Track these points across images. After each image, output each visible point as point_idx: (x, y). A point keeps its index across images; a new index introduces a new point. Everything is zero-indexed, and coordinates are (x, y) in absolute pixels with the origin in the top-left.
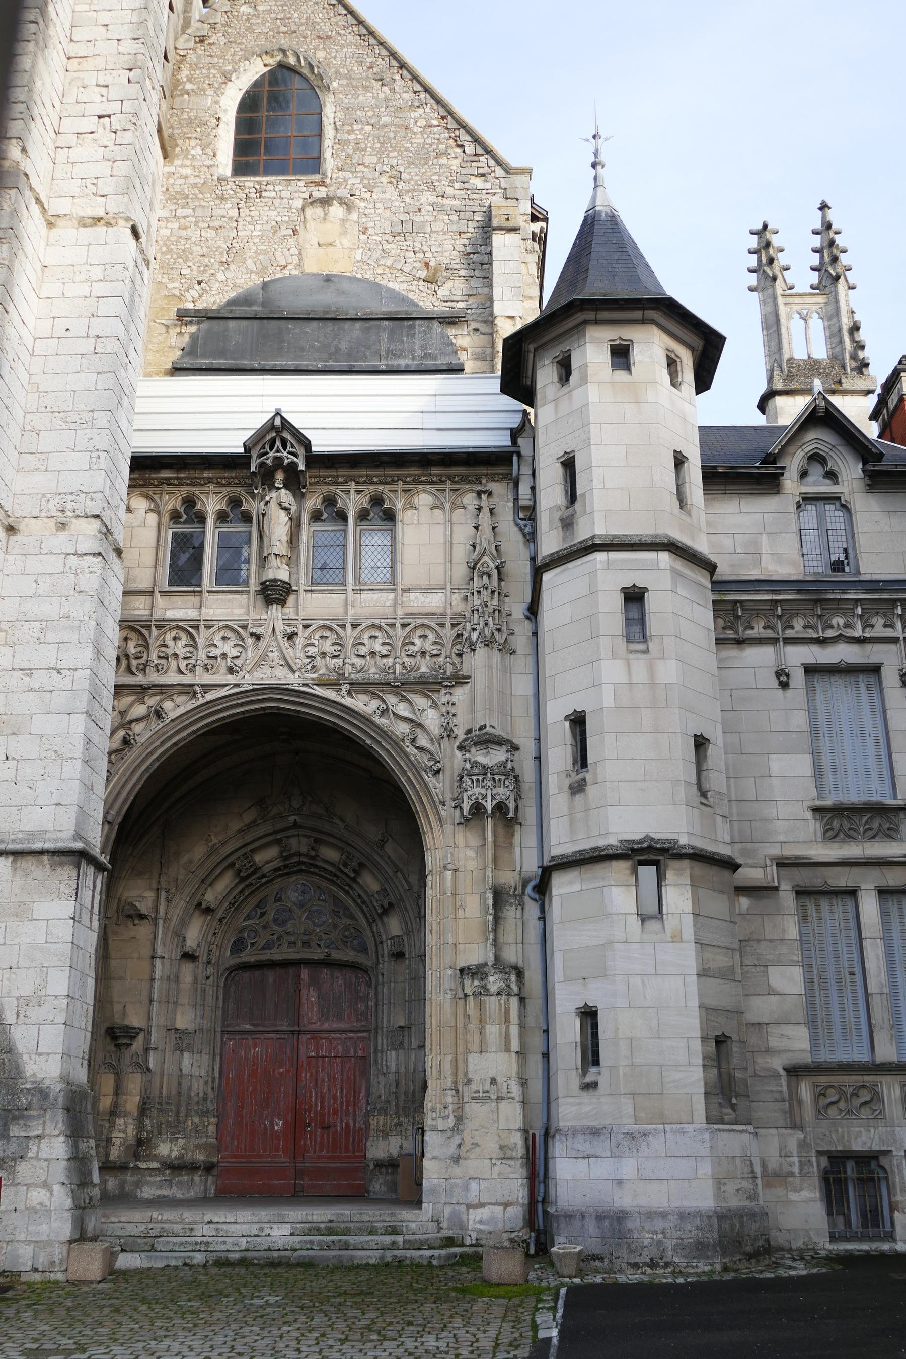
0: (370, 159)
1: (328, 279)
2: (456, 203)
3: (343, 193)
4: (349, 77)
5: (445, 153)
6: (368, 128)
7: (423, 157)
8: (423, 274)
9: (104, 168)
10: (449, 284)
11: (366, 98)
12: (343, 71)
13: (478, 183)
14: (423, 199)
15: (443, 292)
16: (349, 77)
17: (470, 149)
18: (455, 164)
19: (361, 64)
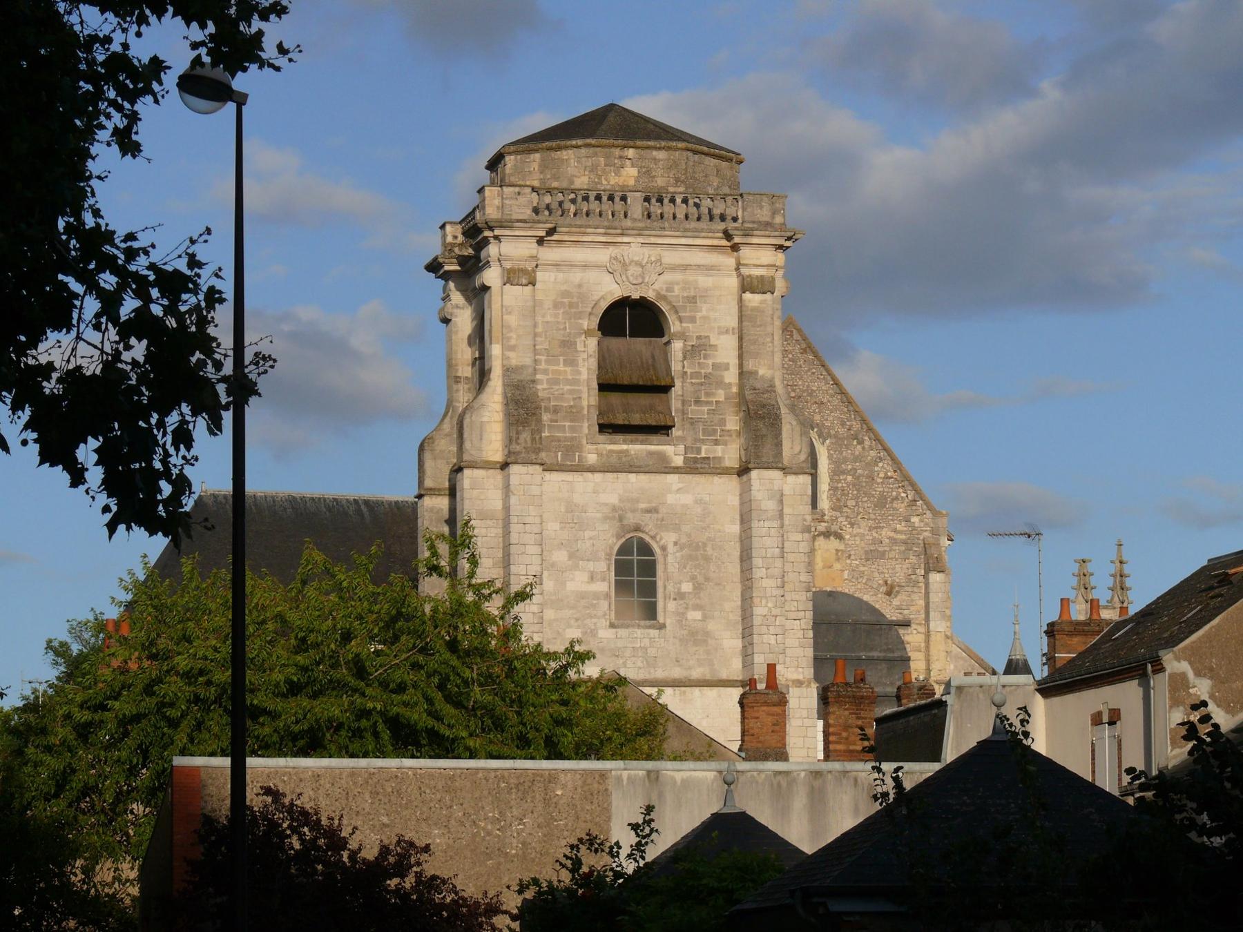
0: (851, 503)
1: (831, 594)
2: (903, 537)
3: (834, 528)
4: (836, 436)
5: (897, 498)
6: (849, 478)
7: (882, 502)
8: (884, 589)
9: (800, 652)
10: (899, 597)
11: (847, 453)
12: (832, 432)
13: (915, 520)
14: (884, 533)
15: (896, 602)
16: (836, 436)
17: (911, 495)
18: (901, 507)
19: (843, 424)
